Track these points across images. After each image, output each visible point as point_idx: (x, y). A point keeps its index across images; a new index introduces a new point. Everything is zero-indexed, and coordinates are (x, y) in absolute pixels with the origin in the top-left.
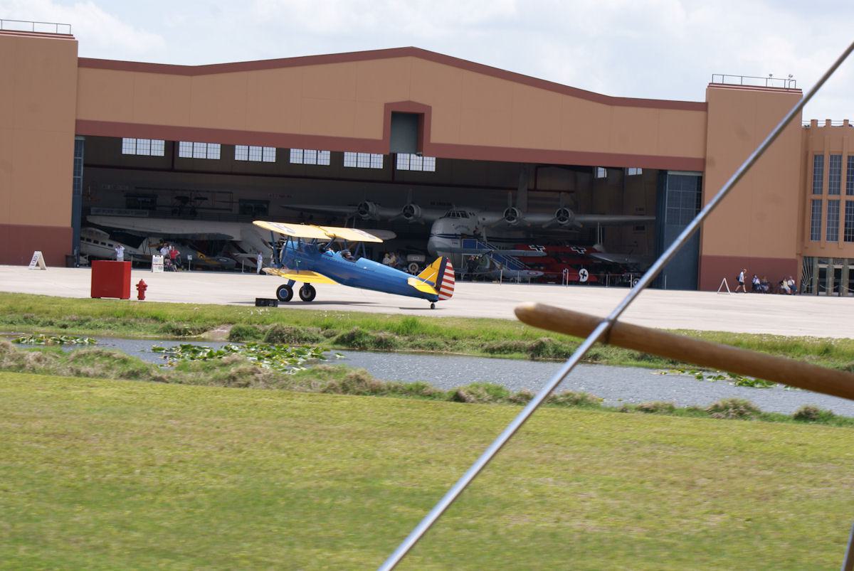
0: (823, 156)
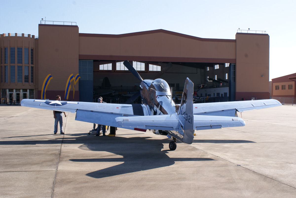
0: (14, 48)
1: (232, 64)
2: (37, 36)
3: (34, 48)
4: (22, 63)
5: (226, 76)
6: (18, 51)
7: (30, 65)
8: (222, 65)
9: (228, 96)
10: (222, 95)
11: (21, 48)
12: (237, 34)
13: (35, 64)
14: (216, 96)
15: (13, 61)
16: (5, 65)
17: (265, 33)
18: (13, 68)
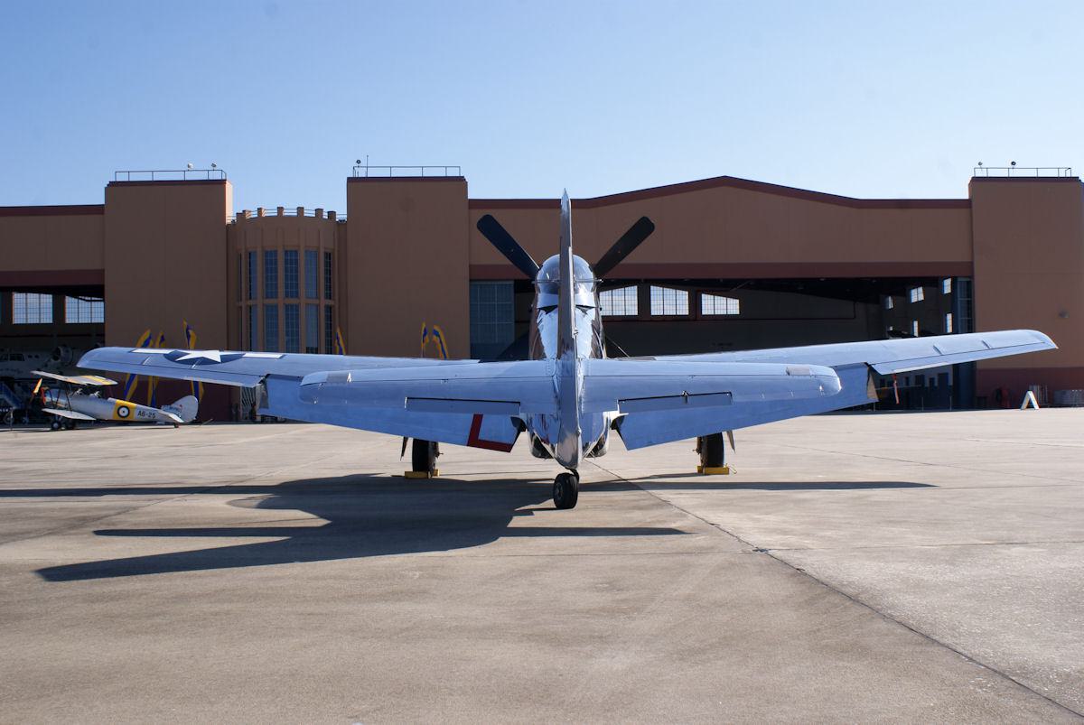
0: (276, 252)
1: (959, 280)
2: (342, 213)
3: (334, 249)
4: (297, 296)
5: (946, 320)
6: (286, 261)
7: (324, 302)
8: (932, 283)
9: (951, 382)
10: (932, 380)
11: (296, 252)
12: (975, 180)
13: (337, 297)
14: (912, 384)
15: (271, 293)
16: (250, 303)
17: (1068, 175)
18: (271, 311)
